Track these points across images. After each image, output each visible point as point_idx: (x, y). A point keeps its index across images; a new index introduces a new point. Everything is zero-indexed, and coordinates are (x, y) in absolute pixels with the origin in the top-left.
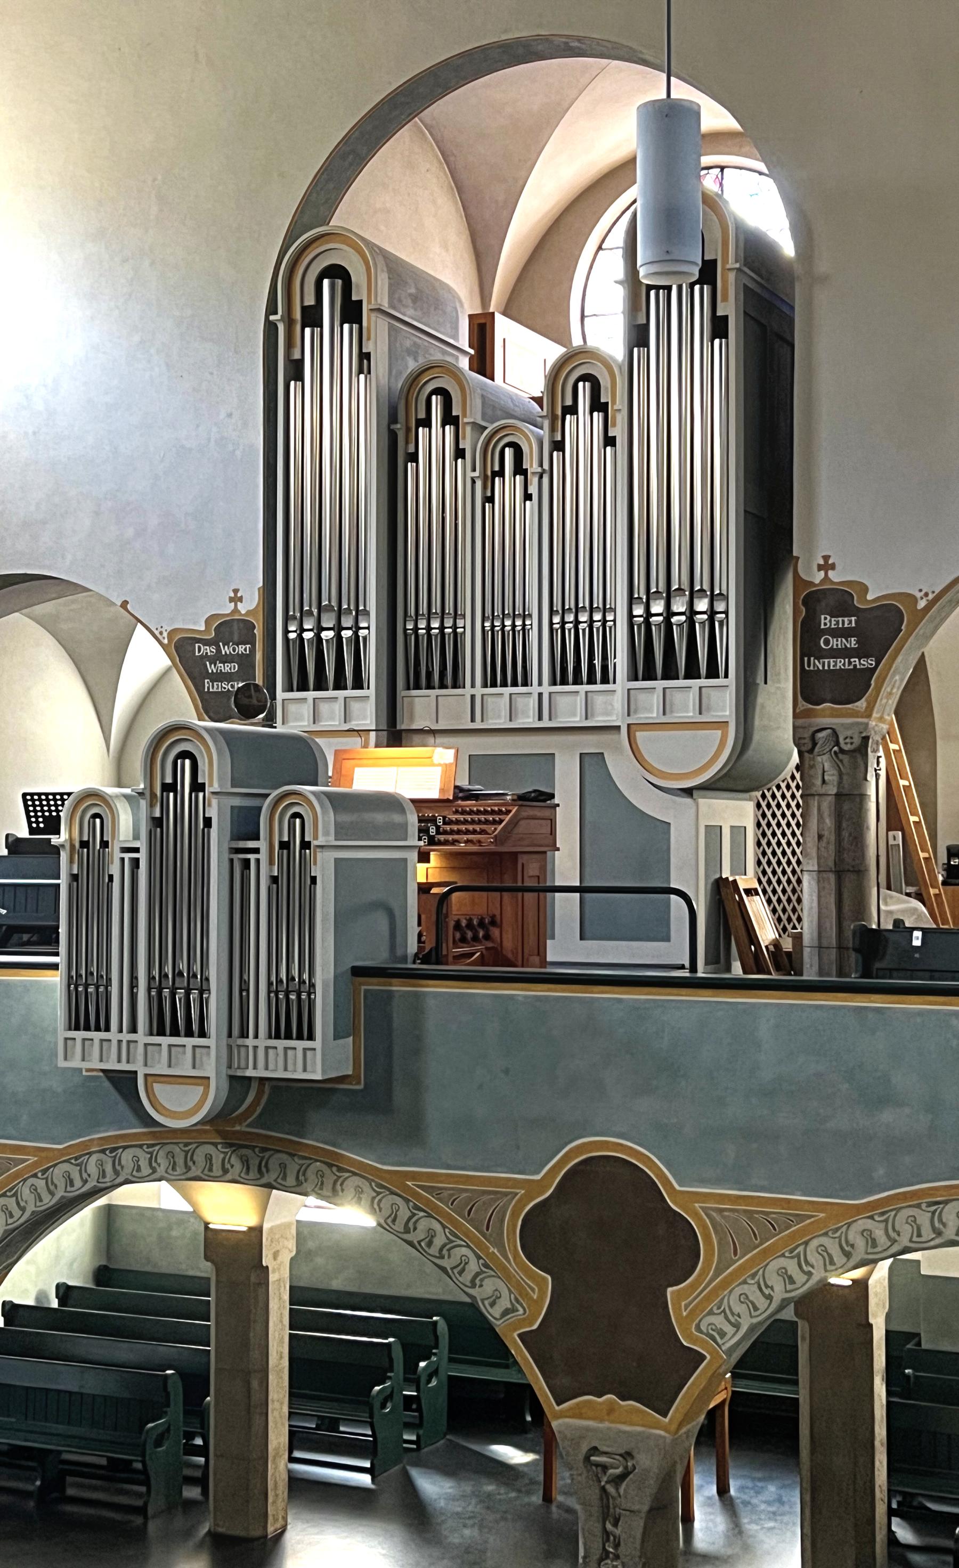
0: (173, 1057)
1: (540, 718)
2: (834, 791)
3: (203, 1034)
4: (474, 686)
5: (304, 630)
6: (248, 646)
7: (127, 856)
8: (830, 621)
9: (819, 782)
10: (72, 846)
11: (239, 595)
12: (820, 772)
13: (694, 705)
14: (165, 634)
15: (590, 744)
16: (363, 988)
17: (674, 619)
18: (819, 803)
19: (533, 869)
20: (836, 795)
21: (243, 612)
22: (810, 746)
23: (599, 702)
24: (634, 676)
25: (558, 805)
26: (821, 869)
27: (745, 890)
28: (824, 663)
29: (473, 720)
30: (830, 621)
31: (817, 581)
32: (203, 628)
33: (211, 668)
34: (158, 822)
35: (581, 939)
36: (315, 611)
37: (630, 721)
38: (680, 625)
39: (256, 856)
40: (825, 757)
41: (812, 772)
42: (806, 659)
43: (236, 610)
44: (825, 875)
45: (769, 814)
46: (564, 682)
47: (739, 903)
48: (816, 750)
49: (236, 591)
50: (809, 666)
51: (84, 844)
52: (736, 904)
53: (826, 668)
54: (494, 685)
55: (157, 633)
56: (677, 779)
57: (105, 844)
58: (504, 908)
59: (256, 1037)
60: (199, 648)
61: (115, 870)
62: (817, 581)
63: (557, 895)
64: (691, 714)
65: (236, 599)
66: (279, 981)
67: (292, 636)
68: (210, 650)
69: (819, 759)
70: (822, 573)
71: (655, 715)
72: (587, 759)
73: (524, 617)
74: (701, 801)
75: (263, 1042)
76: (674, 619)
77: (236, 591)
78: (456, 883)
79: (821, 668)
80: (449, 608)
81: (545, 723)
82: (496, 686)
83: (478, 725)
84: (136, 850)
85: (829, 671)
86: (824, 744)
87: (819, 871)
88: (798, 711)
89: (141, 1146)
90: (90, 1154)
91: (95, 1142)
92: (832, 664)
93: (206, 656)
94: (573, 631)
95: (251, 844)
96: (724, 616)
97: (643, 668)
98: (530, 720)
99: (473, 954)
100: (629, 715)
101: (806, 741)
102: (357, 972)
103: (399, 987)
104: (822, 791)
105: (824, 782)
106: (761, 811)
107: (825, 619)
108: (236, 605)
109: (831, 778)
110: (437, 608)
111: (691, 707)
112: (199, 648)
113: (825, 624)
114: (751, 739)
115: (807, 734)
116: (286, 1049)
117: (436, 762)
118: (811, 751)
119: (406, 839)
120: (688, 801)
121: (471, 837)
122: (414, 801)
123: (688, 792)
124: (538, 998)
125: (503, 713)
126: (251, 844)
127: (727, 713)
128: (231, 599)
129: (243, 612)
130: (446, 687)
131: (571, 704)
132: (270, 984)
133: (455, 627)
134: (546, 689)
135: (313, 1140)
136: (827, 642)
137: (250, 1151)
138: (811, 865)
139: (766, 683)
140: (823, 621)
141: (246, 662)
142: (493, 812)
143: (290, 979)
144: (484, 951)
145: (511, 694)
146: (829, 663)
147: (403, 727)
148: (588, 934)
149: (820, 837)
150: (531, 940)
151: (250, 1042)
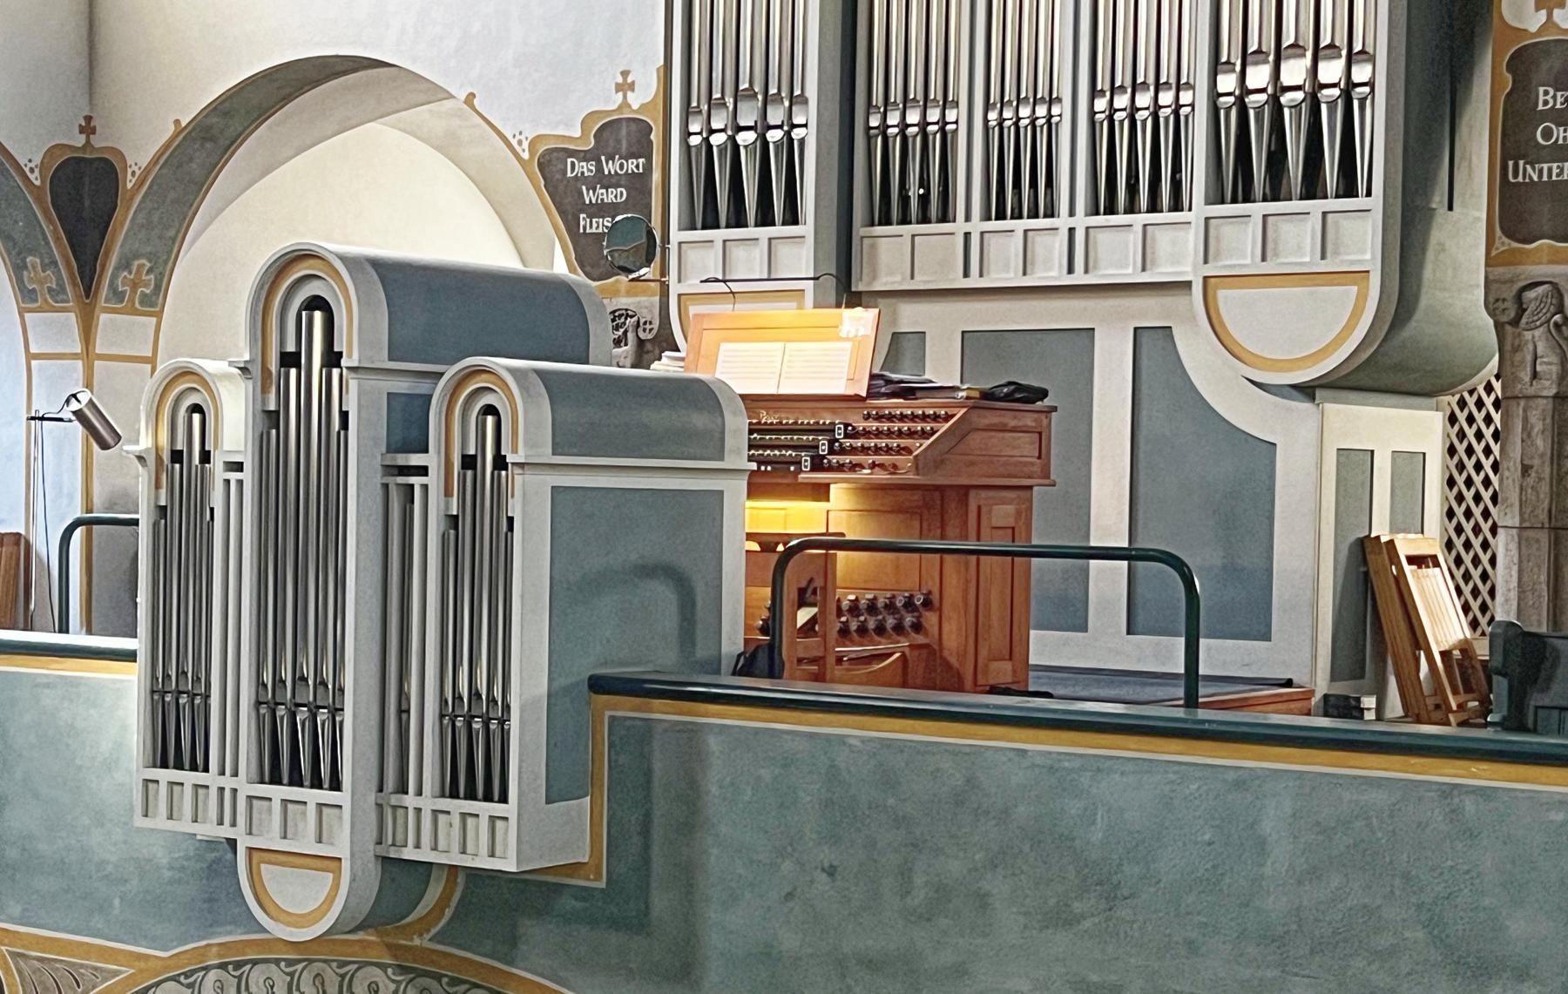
0: (290, 823)
1: (1071, 270)
2: (1553, 391)
3: (336, 785)
4: (969, 222)
5: (712, 132)
6: (641, 161)
7: (234, 476)
8: (1554, 97)
9: (1526, 376)
10: (159, 458)
11: (629, 80)
12: (1529, 358)
13: (1313, 245)
14: (526, 145)
15: (1150, 312)
16: (608, 713)
17: (1285, 99)
18: (1525, 411)
19: (1002, 512)
20: (1556, 397)
21: (635, 107)
22: (1513, 314)
23: (1163, 241)
24: (1217, 196)
25: (1055, 409)
26: (1527, 524)
27: (1412, 560)
28: (1541, 171)
29: (966, 274)
30: (1554, 97)
31: (1533, 29)
32: (578, 134)
33: (589, 197)
34: (273, 419)
35: (1129, 633)
36: (730, 101)
37: (1210, 270)
38: (1296, 107)
39: (423, 480)
40: (1537, 333)
41: (1518, 357)
42: (1511, 163)
43: (625, 104)
44: (1531, 534)
45: (1470, 433)
46: (1111, 209)
47: (1396, 579)
48: (1524, 320)
49: (625, 74)
50: (1516, 175)
51: (176, 456)
52: (1392, 580)
53: (1545, 178)
54: (1001, 216)
55: (514, 142)
56: (1282, 370)
57: (206, 457)
58: (946, 580)
59: (419, 793)
60: (573, 164)
61: (217, 500)
62: (1533, 29)
63: (1034, 560)
64: (1307, 259)
65: (625, 87)
66: (457, 697)
67: (695, 141)
68: (587, 168)
69: (1528, 335)
70: (1544, 12)
71: (1248, 261)
72: (1145, 338)
73: (1051, 102)
74: (1331, 408)
75: (428, 803)
76: (1285, 99)
77: (625, 74)
78: (843, 535)
79: (1535, 178)
80: (935, 91)
81: (1079, 278)
82: (1004, 218)
83: (974, 282)
84: (238, 467)
85: (1550, 181)
86: (1537, 312)
87: (1521, 528)
88: (1494, 253)
89: (277, 962)
90: (207, 969)
91: (214, 949)
92: (1555, 171)
93: (581, 179)
94: (1126, 123)
95: (416, 460)
96: (1367, 89)
97: (1235, 185)
98: (1054, 274)
99: (891, 655)
100: (1206, 262)
101: (1507, 305)
102: (598, 685)
103: (663, 713)
104: (1531, 391)
105: (1535, 375)
106: (1457, 427)
107: (1546, 93)
108: (625, 97)
109: (1545, 367)
110: (915, 90)
111: (1308, 249)
112: (573, 164)
113: (1546, 103)
114: (1417, 298)
115: (1509, 293)
116: (464, 816)
117: (843, 335)
118: (1515, 323)
119: (722, 458)
120: (1306, 406)
121: (879, 459)
122: (742, 396)
123: (1307, 391)
124: (887, 744)
125: (1012, 265)
126: (416, 460)
127: (1368, 256)
128: (619, 88)
129: (635, 107)
130: (929, 222)
131: (1119, 245)
132: (443, 702)
133: (943, 122)
134: (1081, 221)
135: (525, 969)
136: (1547, 134)
137: (435, 983)
138: (1508, 516)
139: (1450, 208)
140: (1541, 98)
141: (638, 185)
142: (924, 417)
143: (475, 694)
144: (907, 651)
145: (1026, 231)
146: (1550, 170)
147: (861, 288)
148: (1140, 618)
149: (1526, 470)
150: (996, 636)
151: (410, 800)
